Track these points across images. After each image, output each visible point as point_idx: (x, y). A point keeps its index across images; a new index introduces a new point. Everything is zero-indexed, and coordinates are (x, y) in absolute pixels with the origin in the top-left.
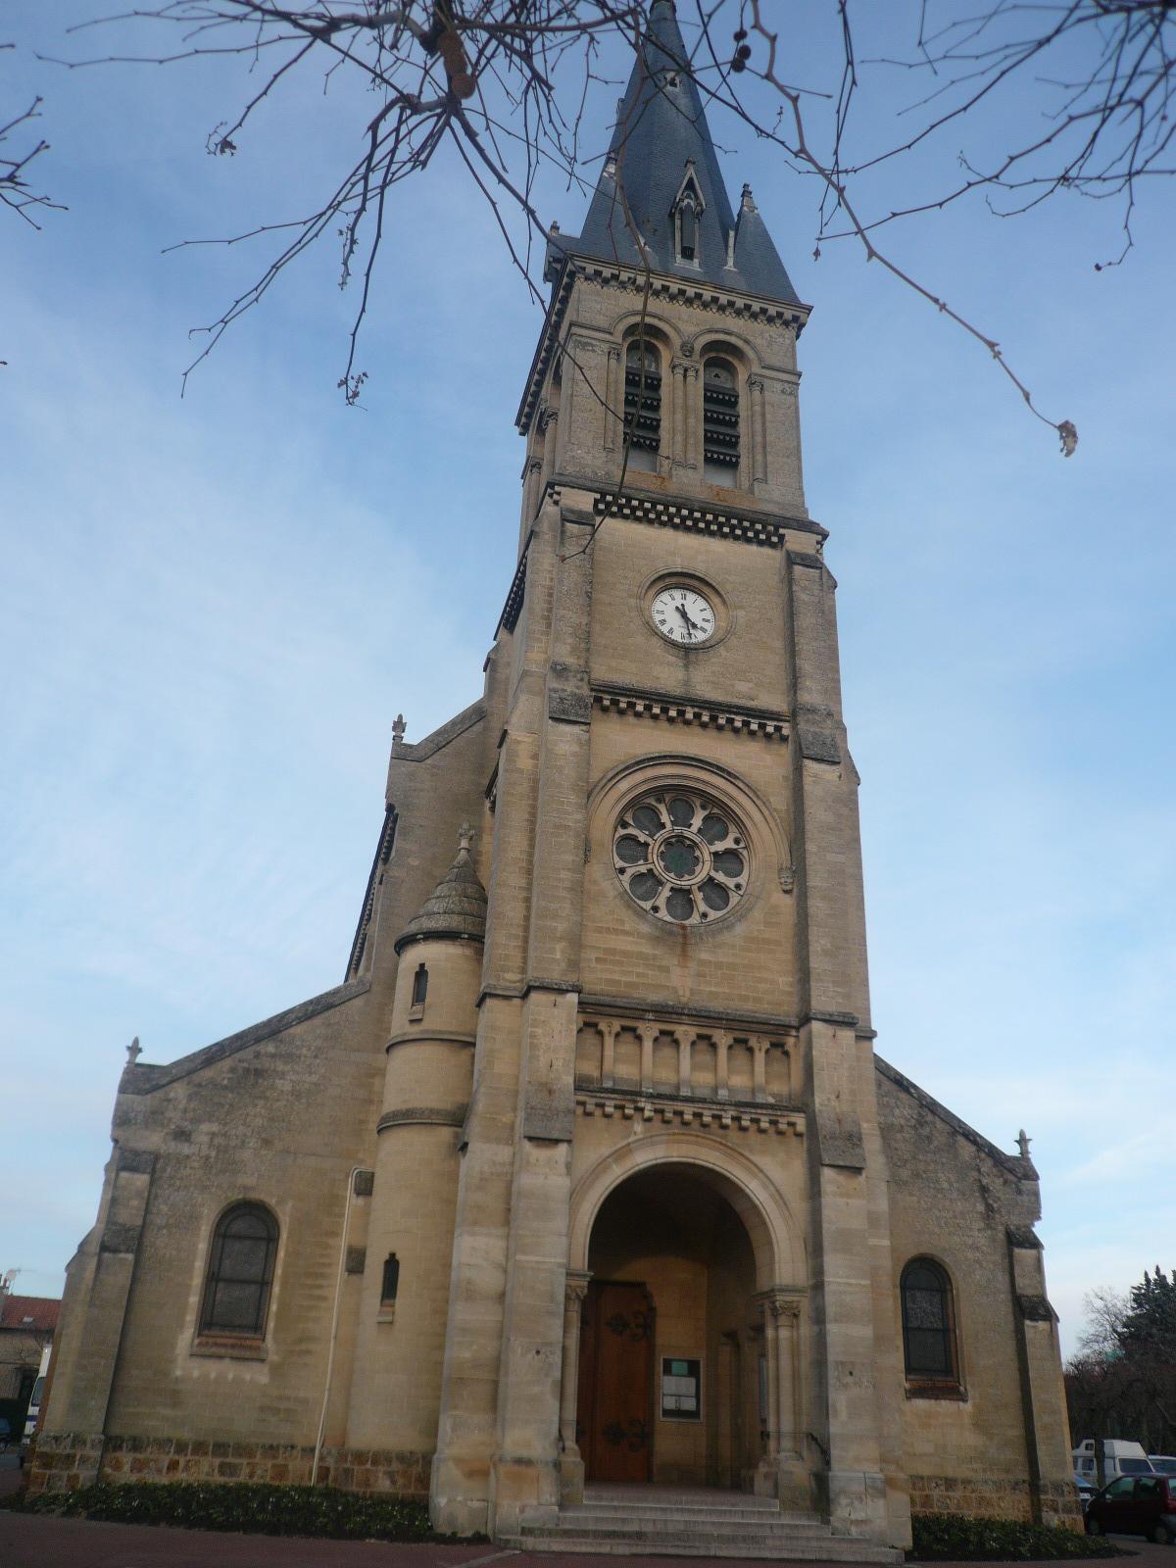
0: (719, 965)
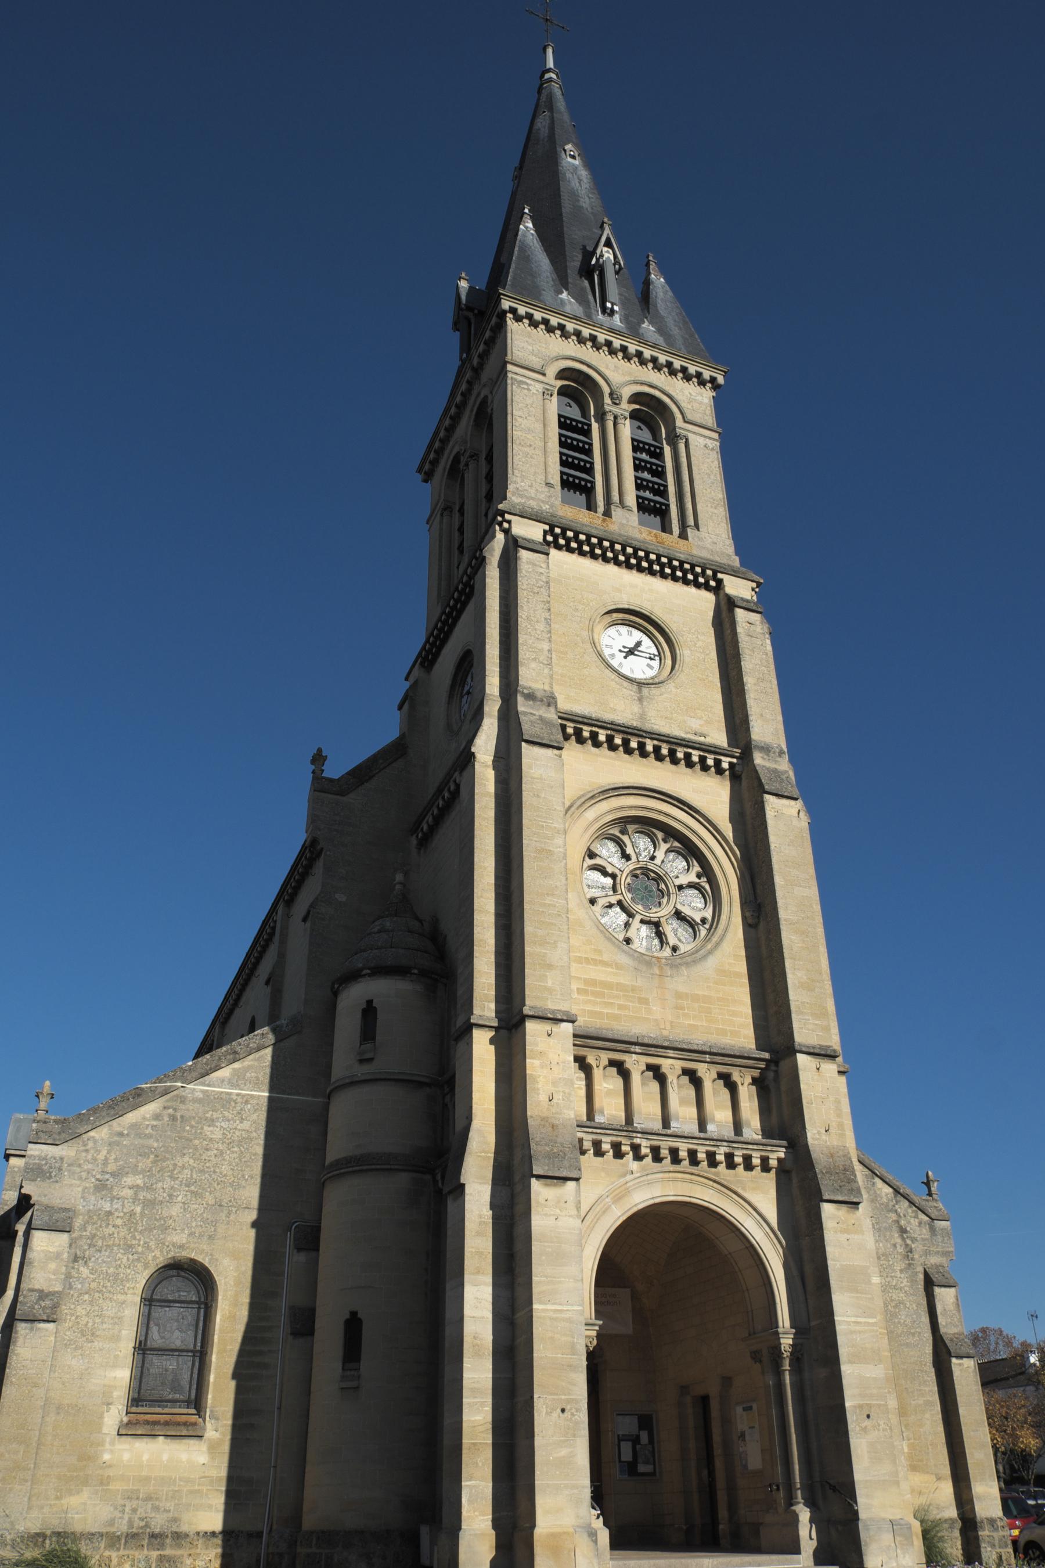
0: (696, 998)
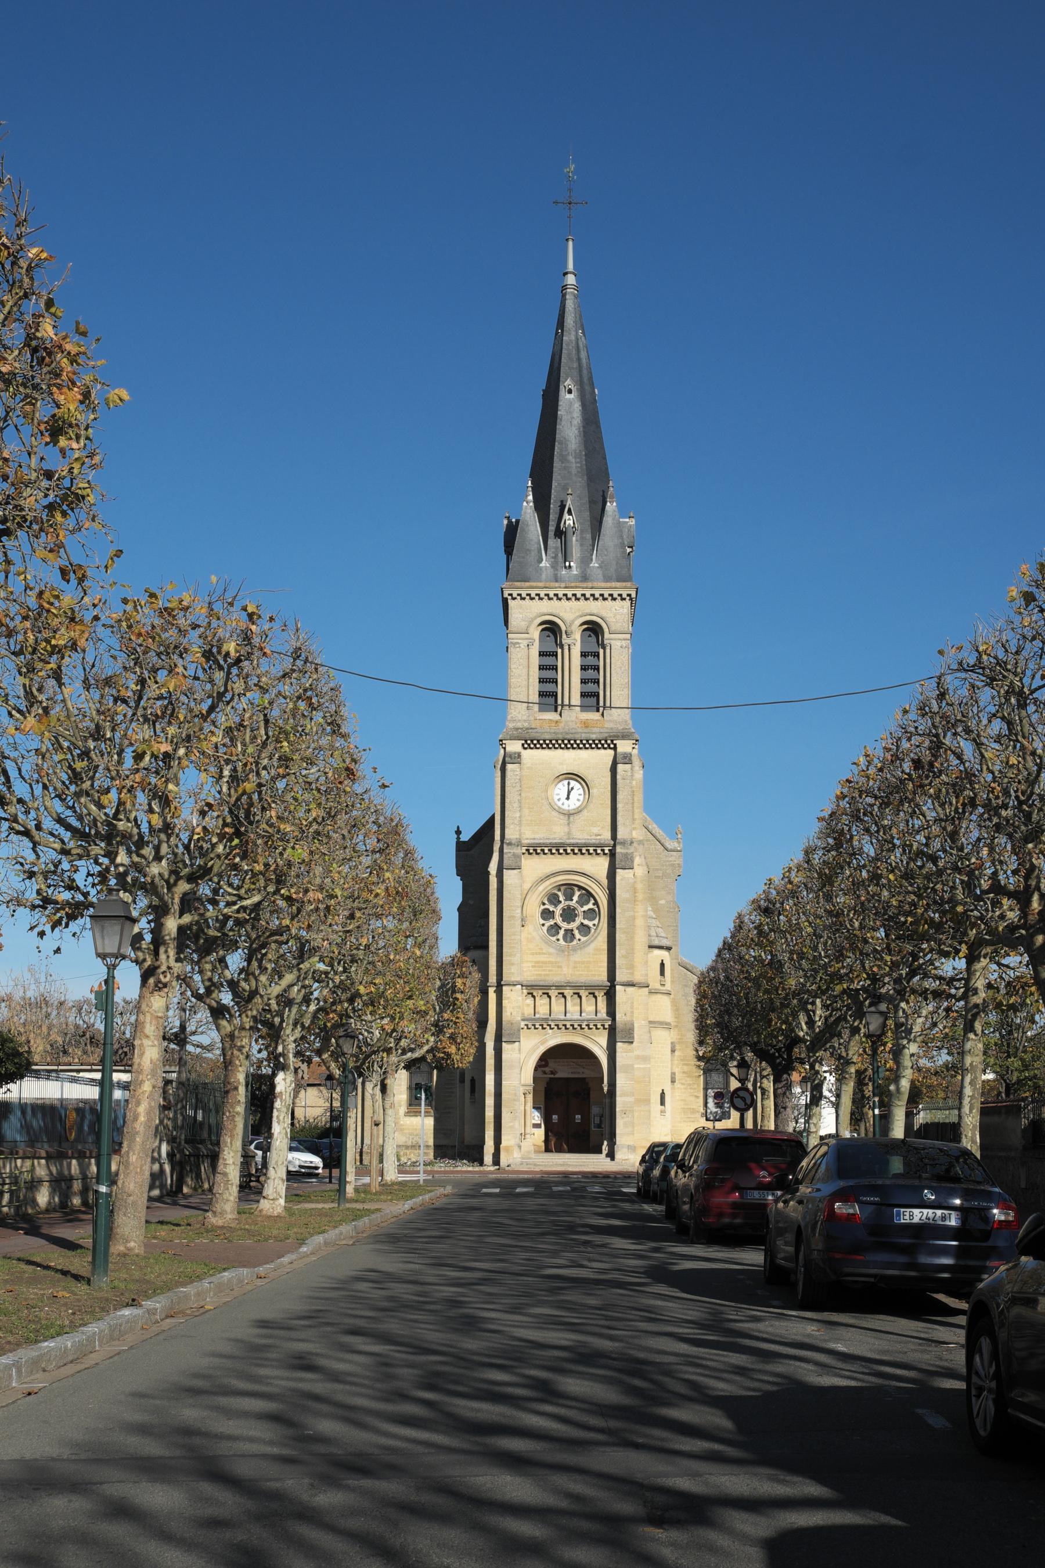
0: (583, 963)
